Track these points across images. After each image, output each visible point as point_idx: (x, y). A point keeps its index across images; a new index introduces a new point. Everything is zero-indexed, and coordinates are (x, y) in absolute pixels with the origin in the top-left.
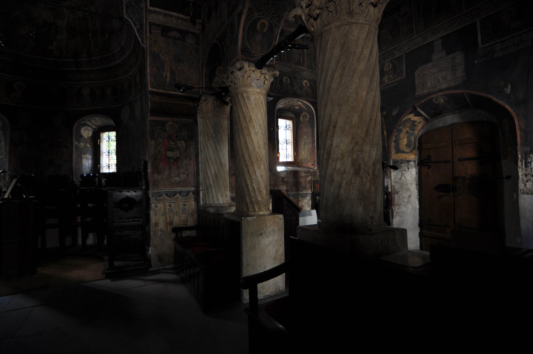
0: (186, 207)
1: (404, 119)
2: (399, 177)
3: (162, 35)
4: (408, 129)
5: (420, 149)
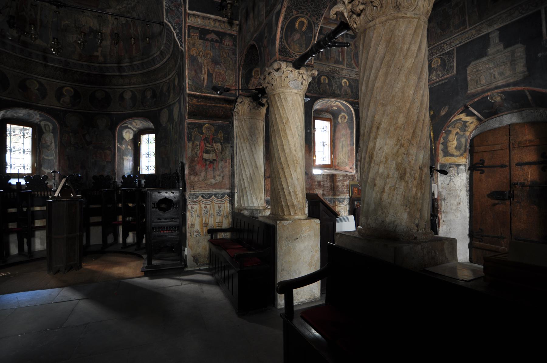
1: (454, 120)
2: (447, 182)
5: (472, 152)
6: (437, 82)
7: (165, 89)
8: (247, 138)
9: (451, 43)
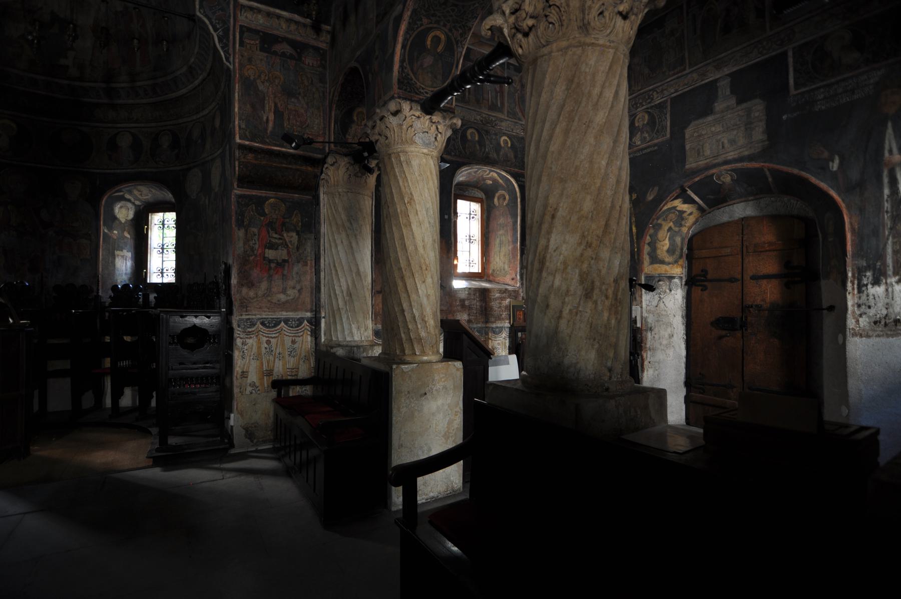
0: (295, 346)
1: (665, 208)
2: (655, 303)
3: (262, 49)
5: (690, 258)
6: (642, 149)
9: (662, 91)
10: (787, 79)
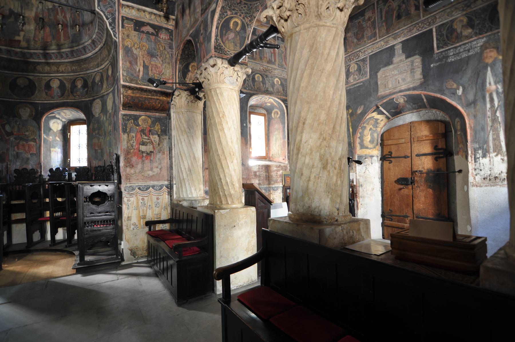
0: (159, 201)
1: (368, 117)
3: (135, 30)
4: (371, 126)
5: (382, 145)
7: (97, 79)
8: (185, 131)
9: (365, 51)
10: (433, 44)
